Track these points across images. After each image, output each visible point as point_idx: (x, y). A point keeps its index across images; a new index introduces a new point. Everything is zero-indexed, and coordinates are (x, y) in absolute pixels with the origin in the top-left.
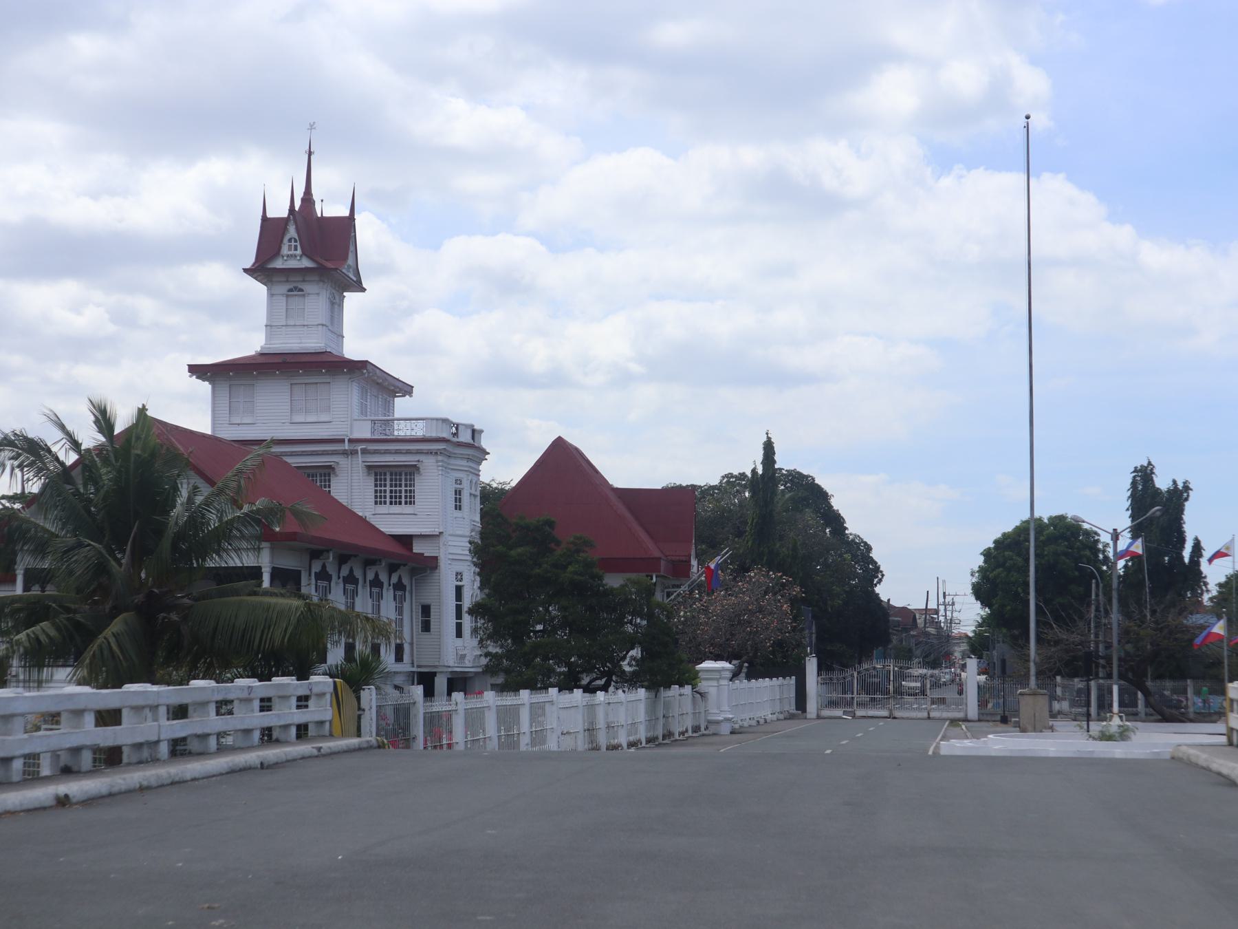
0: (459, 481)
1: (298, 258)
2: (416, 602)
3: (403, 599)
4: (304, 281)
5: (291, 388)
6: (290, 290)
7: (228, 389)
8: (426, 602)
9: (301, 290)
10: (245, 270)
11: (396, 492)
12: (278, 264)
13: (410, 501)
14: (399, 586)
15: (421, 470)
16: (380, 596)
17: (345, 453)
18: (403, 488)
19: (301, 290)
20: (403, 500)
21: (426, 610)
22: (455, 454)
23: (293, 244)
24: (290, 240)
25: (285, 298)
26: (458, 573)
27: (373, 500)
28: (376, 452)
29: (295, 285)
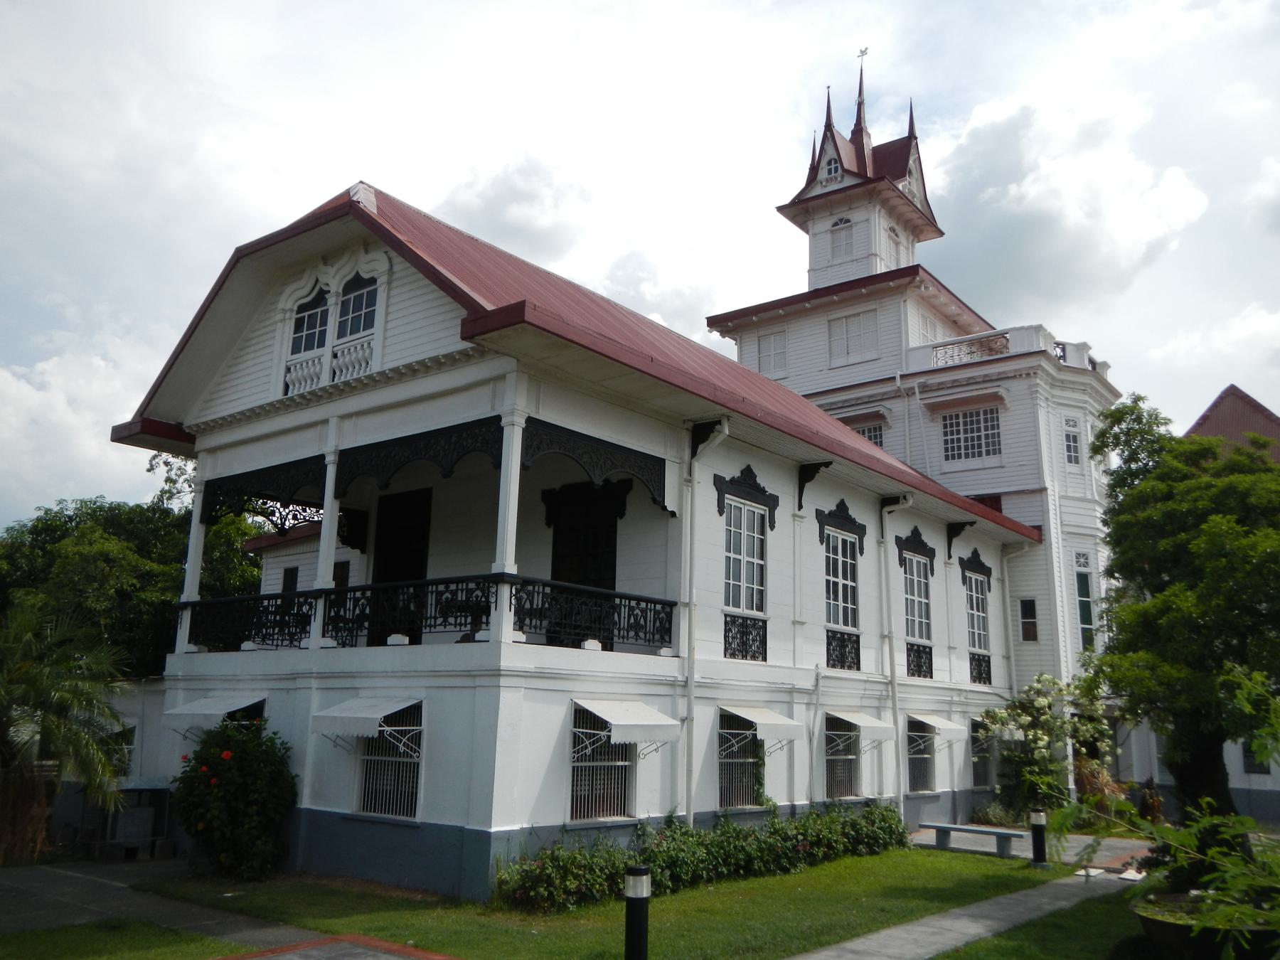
0: (1071, 422)
1: (839, 179)
2: (1011, 597)
3: (983, 588)
4: (851, 209)
5: (829, 326)
6: (835, 224)
7: (757, 342)
8: (1027, 594)
9: (848, 221)
10: (781, 209)
11: (973, 439)
12: (818, 191)
13: (995, 449)
14: (973, 564)
15: (1006, 402)
16: (929, 570)
17: (896, 395)
18: (983, 433)
19: (848, 221)
20: (984, 449)
21: (1028, 608)
22: (1062, 381)
23: (833, 166)
24: (829, 163)
25: (829, 236)
26: (1079, 554)
27: (943, 454)
28: (941, 386)
29: (840, 216)
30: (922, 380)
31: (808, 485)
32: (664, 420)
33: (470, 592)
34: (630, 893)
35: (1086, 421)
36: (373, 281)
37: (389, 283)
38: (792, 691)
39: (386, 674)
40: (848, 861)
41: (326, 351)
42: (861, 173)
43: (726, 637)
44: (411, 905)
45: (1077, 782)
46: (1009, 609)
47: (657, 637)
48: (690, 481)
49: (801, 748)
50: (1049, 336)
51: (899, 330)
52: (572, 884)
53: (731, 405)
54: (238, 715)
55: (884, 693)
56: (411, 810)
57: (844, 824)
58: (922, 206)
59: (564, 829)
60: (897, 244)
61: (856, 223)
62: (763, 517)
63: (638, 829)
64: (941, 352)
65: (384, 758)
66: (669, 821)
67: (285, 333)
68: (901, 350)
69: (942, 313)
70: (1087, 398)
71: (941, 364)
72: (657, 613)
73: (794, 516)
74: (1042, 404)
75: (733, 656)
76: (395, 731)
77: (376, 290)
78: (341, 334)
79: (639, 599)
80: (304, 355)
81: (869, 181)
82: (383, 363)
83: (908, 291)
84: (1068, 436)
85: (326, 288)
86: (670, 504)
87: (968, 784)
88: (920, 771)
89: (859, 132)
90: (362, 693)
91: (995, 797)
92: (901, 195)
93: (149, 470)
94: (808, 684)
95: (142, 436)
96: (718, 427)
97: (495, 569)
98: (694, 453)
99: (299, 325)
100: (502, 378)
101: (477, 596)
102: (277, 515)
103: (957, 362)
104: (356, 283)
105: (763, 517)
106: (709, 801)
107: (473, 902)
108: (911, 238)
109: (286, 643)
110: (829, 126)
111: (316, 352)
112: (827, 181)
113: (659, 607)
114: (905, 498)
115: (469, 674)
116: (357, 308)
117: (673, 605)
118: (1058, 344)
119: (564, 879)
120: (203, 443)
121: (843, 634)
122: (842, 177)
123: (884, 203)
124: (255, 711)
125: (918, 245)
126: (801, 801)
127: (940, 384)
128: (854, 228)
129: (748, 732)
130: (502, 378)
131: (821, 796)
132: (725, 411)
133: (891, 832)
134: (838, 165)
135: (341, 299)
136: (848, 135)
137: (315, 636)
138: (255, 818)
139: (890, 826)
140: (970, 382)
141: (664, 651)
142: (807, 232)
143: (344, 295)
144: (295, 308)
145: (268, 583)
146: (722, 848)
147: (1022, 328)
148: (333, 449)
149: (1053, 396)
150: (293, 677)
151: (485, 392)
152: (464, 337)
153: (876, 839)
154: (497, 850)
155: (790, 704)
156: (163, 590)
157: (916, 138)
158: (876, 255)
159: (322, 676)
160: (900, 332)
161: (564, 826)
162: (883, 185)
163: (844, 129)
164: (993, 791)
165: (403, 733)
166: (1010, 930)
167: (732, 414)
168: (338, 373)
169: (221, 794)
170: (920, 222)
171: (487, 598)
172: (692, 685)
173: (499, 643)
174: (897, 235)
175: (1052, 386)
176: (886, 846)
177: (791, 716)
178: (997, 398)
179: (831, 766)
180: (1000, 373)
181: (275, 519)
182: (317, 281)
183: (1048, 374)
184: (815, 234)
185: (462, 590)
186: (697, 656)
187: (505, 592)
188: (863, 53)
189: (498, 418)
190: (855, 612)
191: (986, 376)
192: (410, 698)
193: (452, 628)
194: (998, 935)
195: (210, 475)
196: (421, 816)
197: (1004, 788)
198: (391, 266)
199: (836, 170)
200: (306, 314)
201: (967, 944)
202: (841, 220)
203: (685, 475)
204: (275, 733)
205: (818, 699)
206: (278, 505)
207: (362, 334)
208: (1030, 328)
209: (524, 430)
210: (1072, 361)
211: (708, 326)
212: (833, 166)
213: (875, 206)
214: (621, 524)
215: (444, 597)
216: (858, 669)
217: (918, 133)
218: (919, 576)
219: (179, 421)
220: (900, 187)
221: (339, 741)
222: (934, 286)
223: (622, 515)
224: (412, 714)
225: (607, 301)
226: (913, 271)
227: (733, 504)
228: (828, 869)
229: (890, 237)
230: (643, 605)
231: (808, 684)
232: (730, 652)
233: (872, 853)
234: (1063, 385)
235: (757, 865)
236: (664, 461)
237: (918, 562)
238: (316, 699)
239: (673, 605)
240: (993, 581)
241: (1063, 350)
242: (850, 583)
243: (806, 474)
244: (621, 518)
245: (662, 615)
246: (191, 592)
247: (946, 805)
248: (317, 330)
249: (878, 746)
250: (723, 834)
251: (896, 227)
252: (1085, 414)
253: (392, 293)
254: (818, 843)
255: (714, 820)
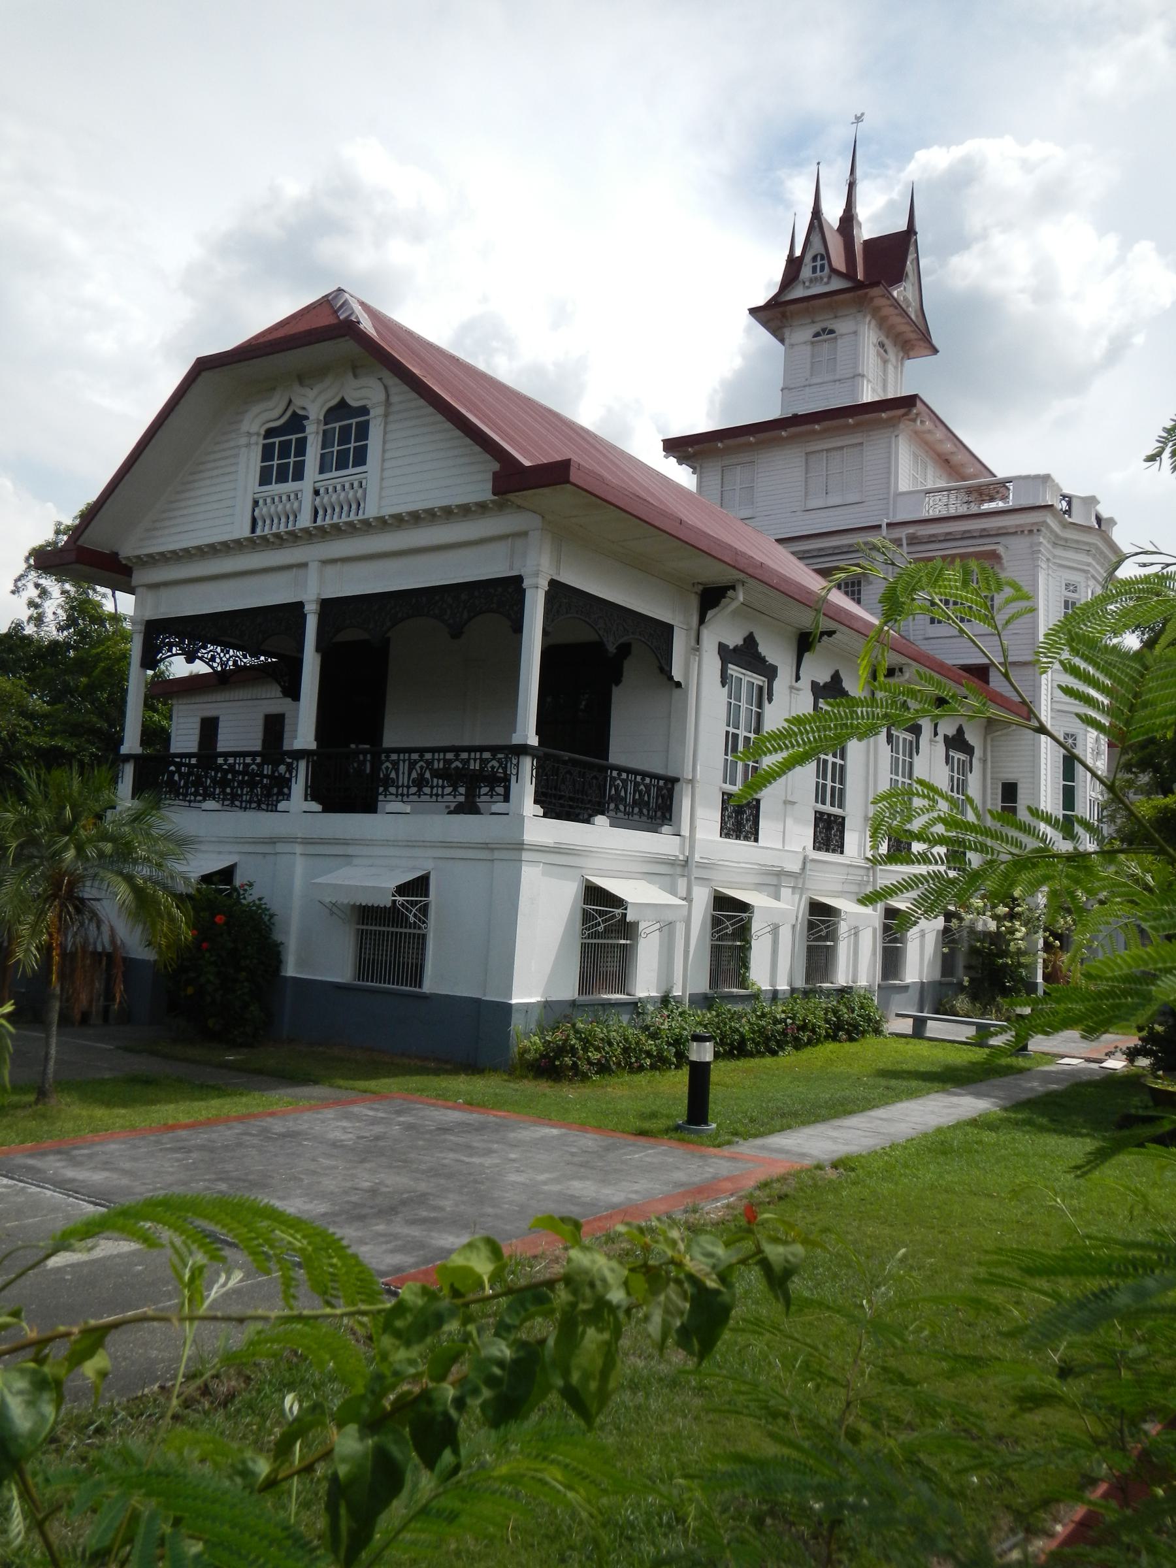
1: (825, 280)
3: (964, 769)
6: (817, 335)
7: (720, 472)
8: (1010, 777)
9: (832, 332)
10: (753, 311)
12: (798, 292)
14: (957, 742)
15: (1004, 561)
19: (832, 332)
22: (1066, 540)
23: (819, 263)
24: (814, 259)
25: (809, 347)
28: (932, 539)
29: (824, 325)
30: (911, 530)
31: (807, 655)
32: (674, 583)
33: (484, 762)
34: (694, 1057)
35: (1088, 586)
36: (364, 411)
37: (386, 415)
38: (781, 874)
39: (386, 843)
40: (831, 1046)
41: (306, 486)
42: (850, 275)
43: (722, 815)
44: (436, 1072)
45: (1046, 978)
46: (989, 791)
47: (659, 814)
48: (698, 650)
49: (785, 935)
50: (1057, 487)
51: (888, 471)
52: (595, 1056)
53: (750, 571)
54: (215, 879)
55: (865, 878)
56: (418, 979)
57: (826, 1011)
58: (917, 316)
59: (573, 1004)
60: (885, 362)
61: (842, 335)
62: (761, 688)
63: (635, 1007)
64: (930, 500)
65: (391, 929)
66: (665, 1000)
67: (251, 462)
68: (888, 493)
69: (934, 451)
70: (1090, 560)
71: (932, 514)
72: (659, 789)
73: (791, 688)
74: (1044, 565)
75: (728, 836)
76: (407, 901)
77: (367, 422)
78: (322, 471)
79: (644, 774)
80: (276, 488)
81: (859, 286)
82: (380, 507)
83: (902, 426)
84: (1066, 602)
85: (301, 412)
86: (677, 675)
87: (937, 976)
88: (892, 960)
89: (848, 219)
90: (356, 861)
91: (961, 988)
92: (896, 304)
93: (13, 592)
94: (795, 867)
95: (78, 566)
96: (730, 593)
97: (516, 740)
98: (702, 621)
99: (267, 453)
100: (523, 534)
101: (493, 767)
102: (218, 660)
103: (952, 511)
104: (341, 410)
105: (761, 688)
106: (701, 985)
107: (495, 1069)
108: (901, 354)
109: (254, 805)
110: (817, 213)
111: (290, 486)
112: (811, 281)
113: (661, 783)
114: (901, 670)
115: (486, 846)
116: (345, 439)
117: (675, 780)
118: (1064, 497)
119: (585, 1050)
120: (139, 577)
121: (829, 815)
122: (830, 277)
123: (875, 312)
124: (227, 874)
125: (908, 363)
126: (783, 986)
127: (931, 536)
128: (839, 341)
129: (744, 915)
130: (523, 534)
131: (800, 983)
132: (742, 576)
133: (869, 1020)
134: (826, 262)
135: (323, 427)
136: (835, 224)
137: (297, 797)
138: (246, 984)
139: (869, 1015)
140: (966, 536)
141: (665, 829)
142: (782, 341)
143: (326, 424)
144: (263, 432)
145: (180, 732)
146: (718, 1028)
147: (1027, 477)
148: (314, 597)
149: (1055, 556)
150: (273, 841)
151: (502, 548)
152: (494, 494)
153: (856, 1026)
154: (518, 1024)
155: (777, 887)
156: (52, 735)
157: (916, 233)
158: (863, 376)
159: (307, 842)
160: (889, 473)
161: (574, 1001)
162: (876, 291)
163: (833, 213)
164: (960, 983)
165: (413, 903)
166: (1013, 1106)
167: (750, 581)
168: (321, 512)
169: (213, 959)
170: (912, 336)
171: (505, 769)
172: (693, 865)
173: (521, 818)
174: (886, 351)
175: (1055, 544)
176: (863, 1033)
177: (778, 898)
178: (994, 556)
179: (811, 951)
180: (1000, 528)
181: (215, 665)
182: (290, 401)
183: (1052, 531)
184: (792, 345)
185: (475, 760)
186: (699, 835)
187: (527, 765)
188: (859, 119)
189: (519, 579)
190: (842, 792)
191: (984, 530)
192: (414, 868)
193: (427, 798)
194: (1006, 1109)
195: (151, 614)
196: (428, 987)
197: (972, 980)
198: (388, 396)
199: (822, 269)
200: (277, 440)
201: (980, 1116)
202: (824, 330)
203: (693, 643)
204: (260, 899)
205: (804, 883)
206: (219, 649)
207: (351, 471)
208: (1037, 477)
209: (547, 593)
210: (1077, 518)
211: (665, 449)
212: (819, 263)
213: (865, 316)
214: (616, 692)
215: (453, 766)
216: (842, 852)
217: (918, 229)
218: (904, 755)
219: (115, 550)
220: (895, 294)
221: (334, 909)
222: (931, 419)
223: (618, 682)
224: (419, 886)
225: (595, 436)
226: (909, 402)
227: (735, 674)
228: (807, 1053)
229: (878, 354)
230: (624, 776)
231: (795, 867)
232: (725, 832)
233: (851, 1039)
234: (1065, 544)
235: (750, 1046)
236: (670, 628)
237: (905, 739)
238: (300, 866)
239: (677, 780)
240: (974, 761)
241: (1069, 503)
242: (839, 761)
243: (804, 643)
244: (617, 684)
245: (665, 791)
246: (131, 743)
247: (914, 995)
248: (292, 460)
249: (856, 932)
250: (718, 1016)
251: (887, 342)
252: (1087, 578)
253: (390, 427)
254: (803, 1028)
255: (705, 1001)
